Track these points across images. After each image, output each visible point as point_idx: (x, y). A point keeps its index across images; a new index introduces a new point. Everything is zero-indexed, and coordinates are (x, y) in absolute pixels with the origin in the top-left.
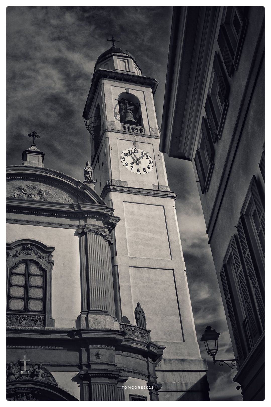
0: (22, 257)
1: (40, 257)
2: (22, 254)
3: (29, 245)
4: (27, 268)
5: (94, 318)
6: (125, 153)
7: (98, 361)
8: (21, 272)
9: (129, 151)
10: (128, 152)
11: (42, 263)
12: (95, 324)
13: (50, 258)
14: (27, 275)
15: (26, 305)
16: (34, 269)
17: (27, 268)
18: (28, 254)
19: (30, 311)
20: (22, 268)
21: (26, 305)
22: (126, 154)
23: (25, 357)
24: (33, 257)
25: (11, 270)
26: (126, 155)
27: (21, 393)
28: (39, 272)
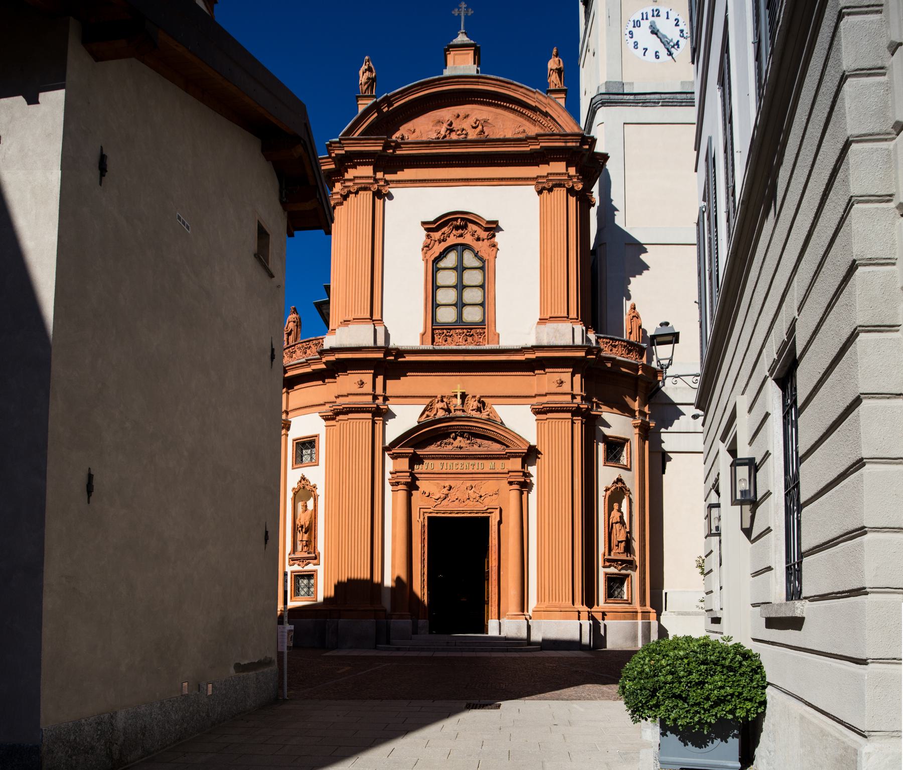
0: (452, 240)
1: (478, 239)
2: (452, 235)
3: (459, 221)
4: (460, 259)
5: (554, 328)
6: (634, 21)
7: (560, 390)
8: (450, 266)
9: (642, 14)
10: (640, 18)
11: (482, 247)
12: (555, 337)
13: (492, 240)
14: (460, 269)
15: (460, 315)
16: (469, 259)
17: (460, 259)
18: (461, 236)
19: (465, 323)
20: (451, 260)
21: (460, 315)
22: (637, 21)
23: (459, 386)
24: (468, 239)
25: (437, 263)
26: (637, 24)
27: (455, 432)
28: (477, 263)
